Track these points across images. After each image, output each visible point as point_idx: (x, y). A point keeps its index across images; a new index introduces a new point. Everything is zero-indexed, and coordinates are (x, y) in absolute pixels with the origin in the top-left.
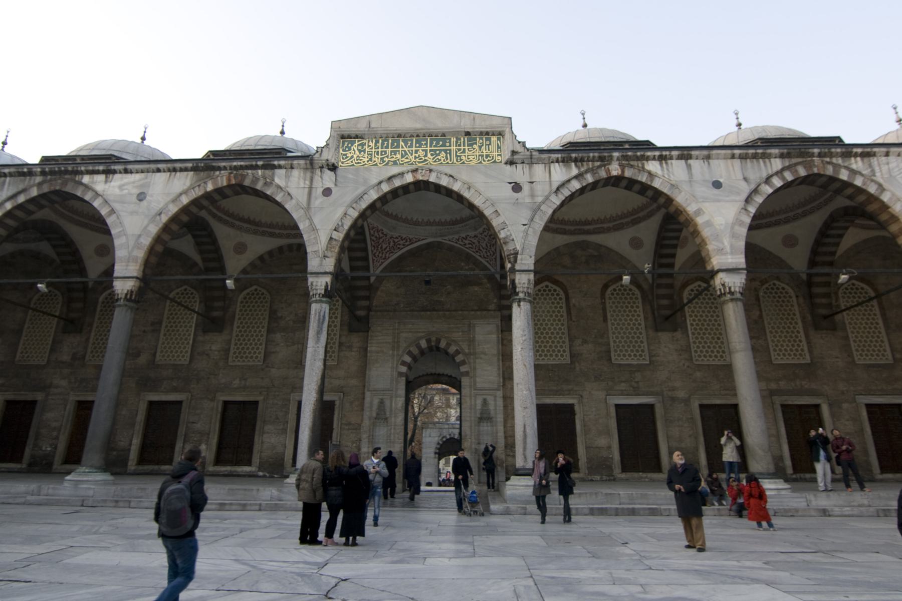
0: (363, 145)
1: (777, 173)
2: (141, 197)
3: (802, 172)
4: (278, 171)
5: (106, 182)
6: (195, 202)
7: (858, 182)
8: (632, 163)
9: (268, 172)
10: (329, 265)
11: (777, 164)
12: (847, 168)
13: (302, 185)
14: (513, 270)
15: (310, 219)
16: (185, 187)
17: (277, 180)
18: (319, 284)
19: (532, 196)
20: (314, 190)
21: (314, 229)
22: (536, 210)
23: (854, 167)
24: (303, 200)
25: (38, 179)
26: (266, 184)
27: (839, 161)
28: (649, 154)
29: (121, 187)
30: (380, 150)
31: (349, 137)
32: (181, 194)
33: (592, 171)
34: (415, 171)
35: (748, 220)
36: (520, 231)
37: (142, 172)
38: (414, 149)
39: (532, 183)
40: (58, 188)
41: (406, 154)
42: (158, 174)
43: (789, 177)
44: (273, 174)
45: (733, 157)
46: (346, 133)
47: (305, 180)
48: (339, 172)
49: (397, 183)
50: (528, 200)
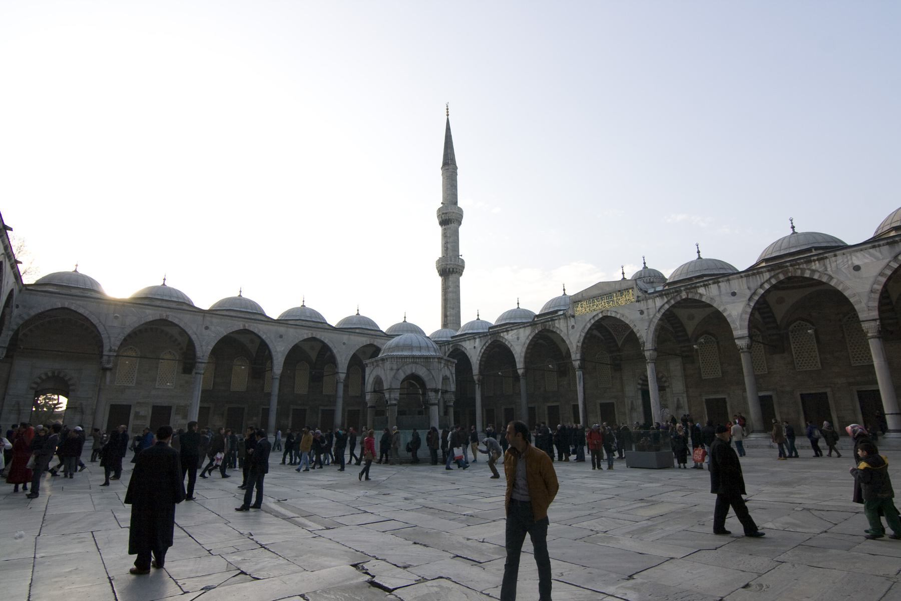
1: (767, 281)
2: (518, 338)
3: (782, 277)
6: (534, 337)
7: (816, 277)
10: (578, 356)
11: (767, 276)
12: (809, 269)
14: (644, 350)
17: (557, 325)
18: (577, 364)
19: (648, 315)
22: (651, 321)
23: (814, 268)
27: (805, 266)
33: (673, 298)
35: (750, 310)
36: (645, 332)
43: (774, 281)
49: (596, 319)
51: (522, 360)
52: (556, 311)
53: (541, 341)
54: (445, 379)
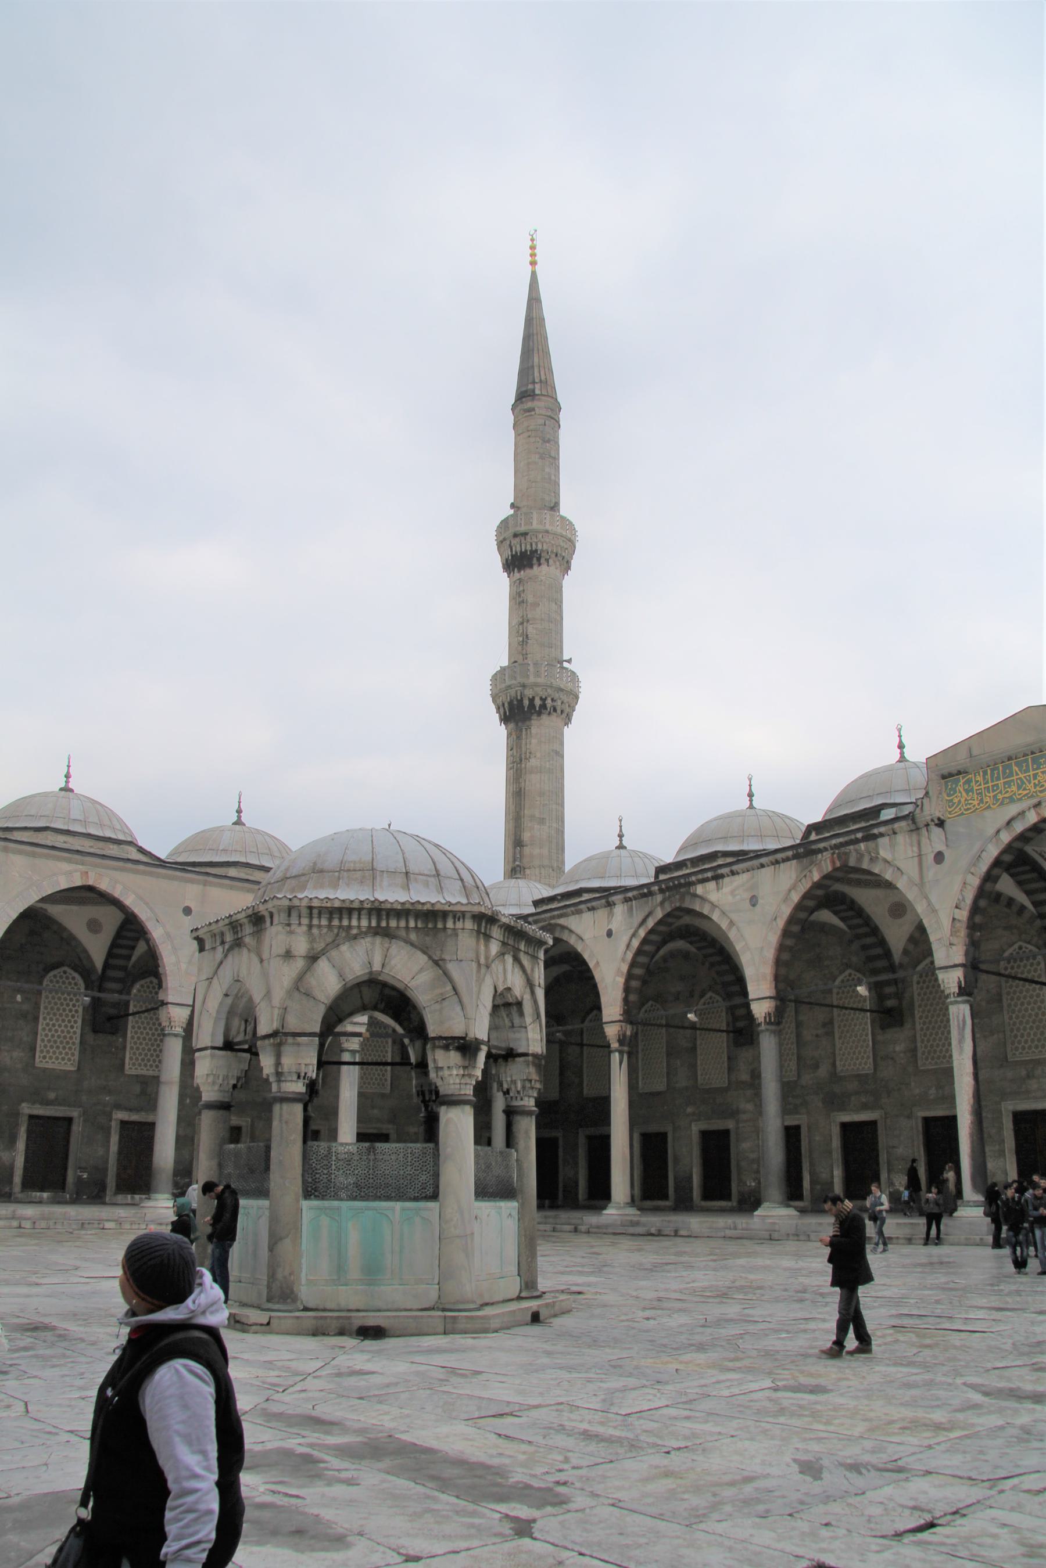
0: (969, 782)
2: (754, 901)
4: (880, 840)
5: (718, 889)
6: (806, 896)
9: (871, 844)
10: (958, 955)
15: (926, 897)
16: (793, 881)
17: (883, 853)
18: (951, 980)
20: (924, 858)
21: (934, 911)
24: (914, 873)
25: (659, 898)
29: (732, 893)
30: (990, 784)
31: (951, 775)
32: (790, 891)
34: (1038, 805)
38: (1031, 773)
40: (678, 905)
41: (1023, 782)
42: (763, 870)
44: (877, 846)
46: (945, 772)
47: (912, 846)
48: (947, 825)
49: (1019, 827)
51: (767, 970)
52: (876, 810)
53: (826, 916)
54: (505, 1006)
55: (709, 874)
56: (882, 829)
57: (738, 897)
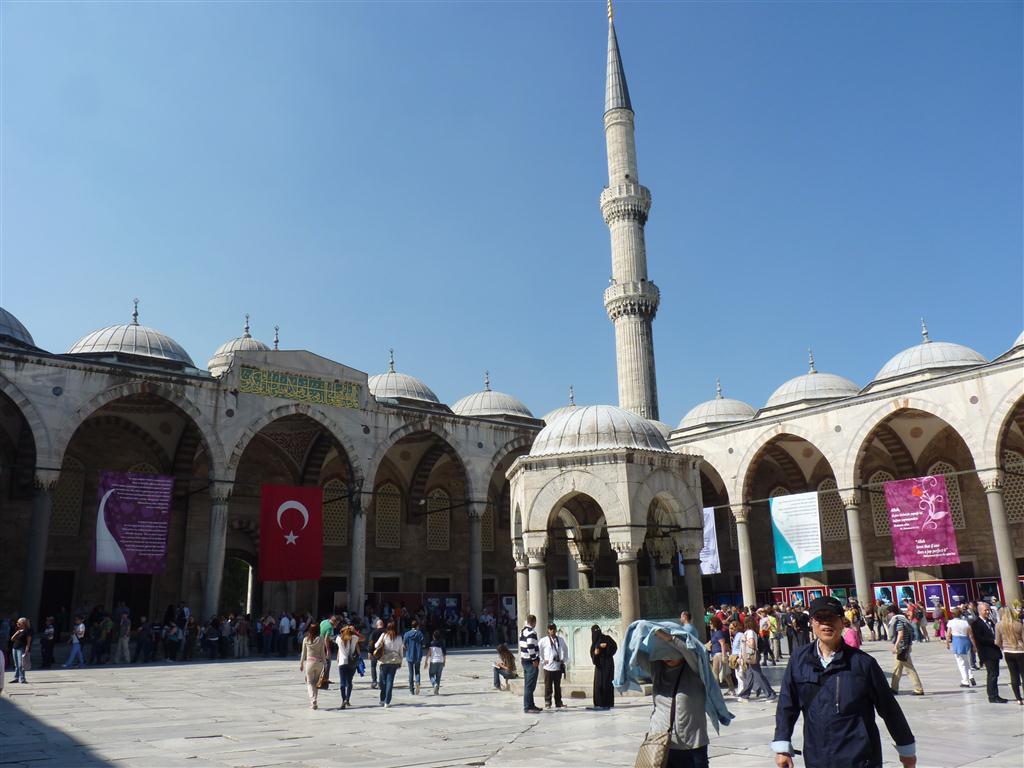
0: (258, 375)
2: (57, 391)
4: (187, 387)
8: (437, 422)
13: (209, 403)
15: (216, 434)
16: (102, 389)
18: (225, 490)
19: (376, 437)
21: (220, 444)
22: (377, 448)
26: (177, 397)
28: (448, 418)
29: (34, 378)
32: (98, 395)
33: (413, 424)
36: (366, 463)
37: (56, 366)
39: (376, 427)
45: (491, 428)
46: (246, 364)
48: (240, 395)
49: (284, 413)
50: (373, 441)
55: (12, 355)
56: (193, 381)
57: (40, 383)
